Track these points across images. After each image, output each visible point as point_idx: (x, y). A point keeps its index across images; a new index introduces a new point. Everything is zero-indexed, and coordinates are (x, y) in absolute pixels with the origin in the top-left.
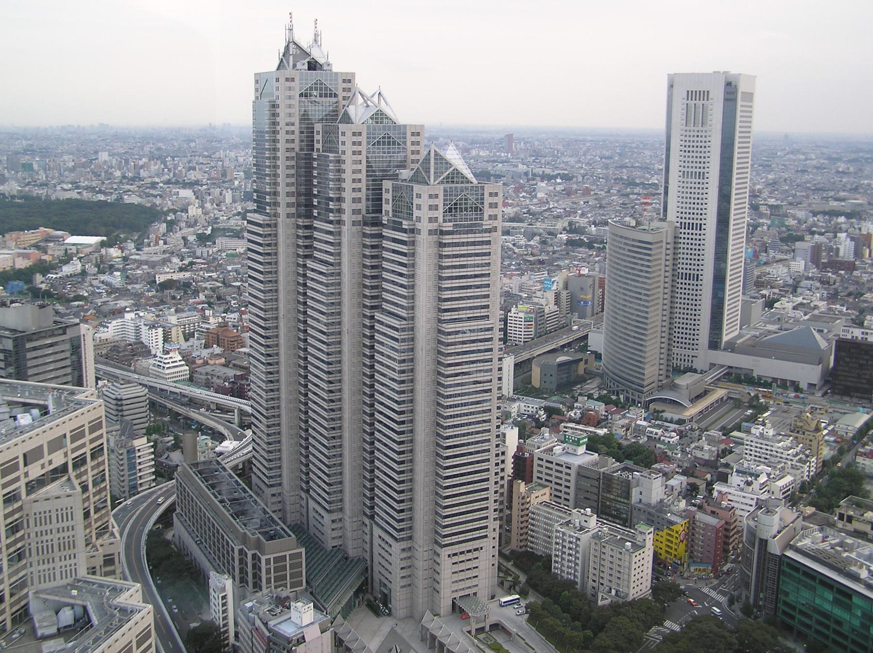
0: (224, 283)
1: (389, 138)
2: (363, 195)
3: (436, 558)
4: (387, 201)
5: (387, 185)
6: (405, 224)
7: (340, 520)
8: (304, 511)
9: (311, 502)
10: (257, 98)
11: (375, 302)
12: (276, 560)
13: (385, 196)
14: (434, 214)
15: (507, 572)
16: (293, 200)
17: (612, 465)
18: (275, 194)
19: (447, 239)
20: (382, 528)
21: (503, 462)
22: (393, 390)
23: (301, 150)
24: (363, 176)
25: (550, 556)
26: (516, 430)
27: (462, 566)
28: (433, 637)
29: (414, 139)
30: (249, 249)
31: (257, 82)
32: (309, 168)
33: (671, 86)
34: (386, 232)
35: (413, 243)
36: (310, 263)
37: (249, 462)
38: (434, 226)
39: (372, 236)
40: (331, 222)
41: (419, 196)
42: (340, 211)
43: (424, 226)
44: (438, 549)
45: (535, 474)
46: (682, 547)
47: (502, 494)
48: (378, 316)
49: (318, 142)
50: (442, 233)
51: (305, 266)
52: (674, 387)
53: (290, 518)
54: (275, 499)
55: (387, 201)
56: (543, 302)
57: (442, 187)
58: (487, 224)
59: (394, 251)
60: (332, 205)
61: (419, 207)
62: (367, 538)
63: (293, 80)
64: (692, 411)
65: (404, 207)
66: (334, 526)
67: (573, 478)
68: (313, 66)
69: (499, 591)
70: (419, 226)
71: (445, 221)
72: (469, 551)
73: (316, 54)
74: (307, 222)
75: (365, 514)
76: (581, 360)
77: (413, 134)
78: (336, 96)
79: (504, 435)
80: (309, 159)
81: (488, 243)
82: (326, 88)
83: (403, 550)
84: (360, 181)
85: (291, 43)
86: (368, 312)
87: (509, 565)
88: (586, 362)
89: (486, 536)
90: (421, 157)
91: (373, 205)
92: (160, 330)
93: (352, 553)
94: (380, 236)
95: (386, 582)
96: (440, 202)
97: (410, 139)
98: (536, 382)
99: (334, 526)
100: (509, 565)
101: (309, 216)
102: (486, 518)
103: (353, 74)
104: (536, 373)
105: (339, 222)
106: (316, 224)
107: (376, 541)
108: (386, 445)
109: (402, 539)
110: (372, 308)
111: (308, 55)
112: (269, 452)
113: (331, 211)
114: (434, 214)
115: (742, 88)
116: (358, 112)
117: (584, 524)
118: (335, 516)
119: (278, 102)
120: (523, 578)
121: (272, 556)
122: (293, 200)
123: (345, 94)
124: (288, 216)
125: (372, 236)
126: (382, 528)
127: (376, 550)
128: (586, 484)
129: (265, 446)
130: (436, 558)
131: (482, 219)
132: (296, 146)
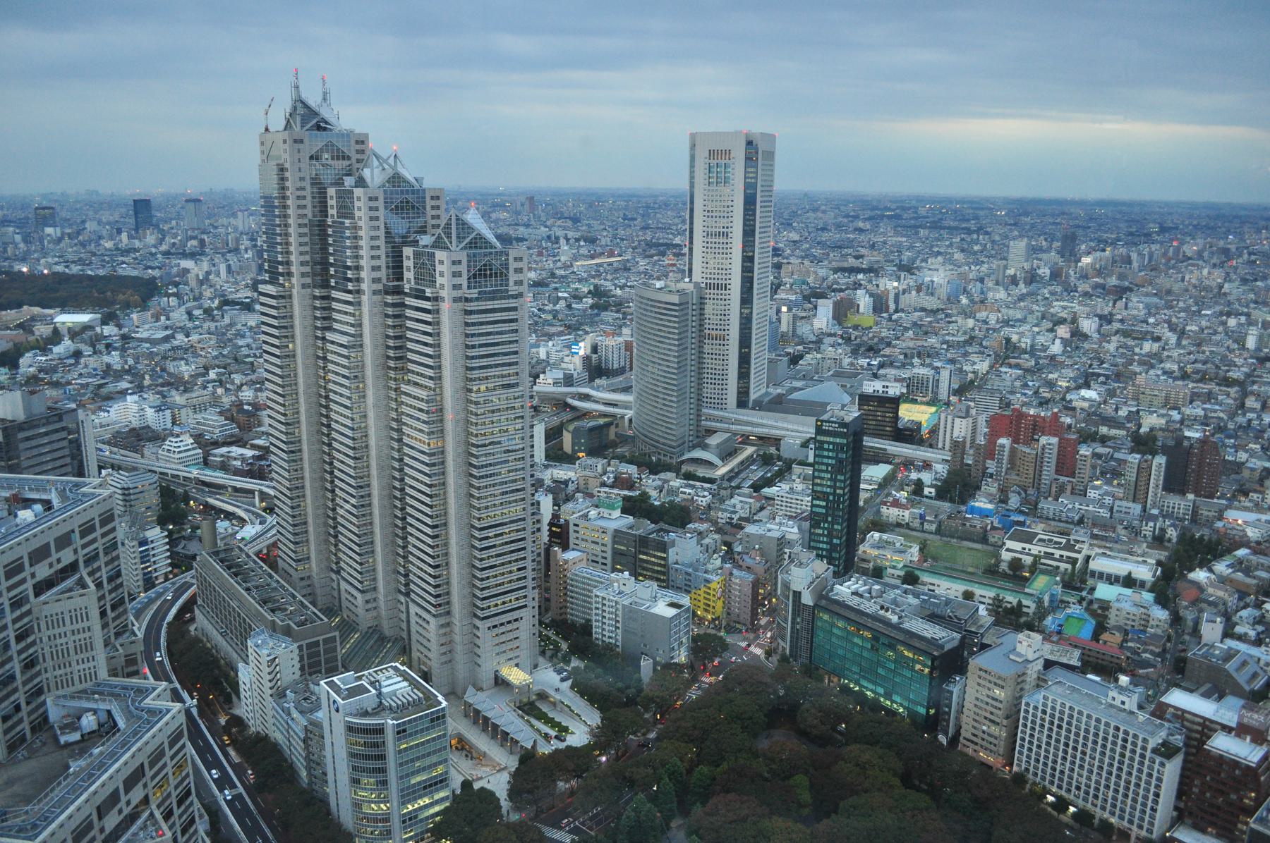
0: (236, 359)
2: (382, 262)
4: (408, 269)
5: (408, 251)
6: (429, 292)
7: (375, 600)
8: (336, 594)
9: (343, 584)
10: (263, 161)
12: (309, 646)
13: (406, 263)
14: (457, 281)
16: (307, 269)
17: (647, 527)
18: (288, 263)
19: (473, 306)
20: (418, 605)
21: (539, 530)
22: (423, 463)
23: (314, 216)
24: (381, 242)
25: (590, 620)
26: (550, 497)
27: (503, 638)
28: (477, 712)
29: (434, 203)
30: (263, 323)
31: (262, 143)
32: (323, 236)
33: (693, 147)
34: (409, 301)
35: (438, 311)
36: (329, 336)
37: (275, 545)
38: (458, 293)
39: (394, 305)
40: (349, 292)
41: (441, 262)
42: (358, 280)
44: (478, 623)
45: (572, 540)
46: (720, 603)
47: (539, 562)
48: (404, 388)
49: (332, 207)
50: (467, 300)
51: (324, 339)
52: (705, 447)
53: (321, 601)
54: (304, 583)
55: (409, 268)
56: (571, 366)
57: (465, 253)
58: (513, 289)
59: (418, 320)
60: (350, 274)
61: (442, 274)
62: (404, 617)
63: (301, 141)
65: (426, 273)
66: (369, 606)
68: (321, 126)
69: (541, 660)
70: (444, 293)
71: (469, 288)
73: (325, 113)
74: (324, 292)
75: (400, 592)
77: (432, 198)
78: (349, 158)
79: (538, 503)
80: (322, 226)
81: (515, 309)
82: (338, 150)
83: (442, 626)
84: (378, 248)
85: (300, 102)
90: (443, 222)
91: (394, 274)
92: (168, 412)
93: (387, 632)
94: (403, 305)
95: (426, 660)
96: (463, 268)
97: (429, 203)
98: (567, 446)
99: (369, 606)
100: (551, 633)
101: (325, 284)
102: (525, 587)
103: (366, 136)
104: (567, 438)
105: (358, 292)
106: (335, 294)
107: (413, 619)
108: (418, 520)
109: (440, 615)
111: (316, 114)
112: (295, 534)
113: (350, 280)
114: (457, 281)
116: (374, 175)
117: (623, 588)
118: (369, 596)
119: (287, 165)
120: (564, 646)
121: (304, 643)
122: (307, 269)
123: (359, 156)
124: (304, 286)
125: (394, 305)
126: (418, 605)
127: (414, 627)
129: (290, 529)
131: (507, 285)
132: (309, 212)
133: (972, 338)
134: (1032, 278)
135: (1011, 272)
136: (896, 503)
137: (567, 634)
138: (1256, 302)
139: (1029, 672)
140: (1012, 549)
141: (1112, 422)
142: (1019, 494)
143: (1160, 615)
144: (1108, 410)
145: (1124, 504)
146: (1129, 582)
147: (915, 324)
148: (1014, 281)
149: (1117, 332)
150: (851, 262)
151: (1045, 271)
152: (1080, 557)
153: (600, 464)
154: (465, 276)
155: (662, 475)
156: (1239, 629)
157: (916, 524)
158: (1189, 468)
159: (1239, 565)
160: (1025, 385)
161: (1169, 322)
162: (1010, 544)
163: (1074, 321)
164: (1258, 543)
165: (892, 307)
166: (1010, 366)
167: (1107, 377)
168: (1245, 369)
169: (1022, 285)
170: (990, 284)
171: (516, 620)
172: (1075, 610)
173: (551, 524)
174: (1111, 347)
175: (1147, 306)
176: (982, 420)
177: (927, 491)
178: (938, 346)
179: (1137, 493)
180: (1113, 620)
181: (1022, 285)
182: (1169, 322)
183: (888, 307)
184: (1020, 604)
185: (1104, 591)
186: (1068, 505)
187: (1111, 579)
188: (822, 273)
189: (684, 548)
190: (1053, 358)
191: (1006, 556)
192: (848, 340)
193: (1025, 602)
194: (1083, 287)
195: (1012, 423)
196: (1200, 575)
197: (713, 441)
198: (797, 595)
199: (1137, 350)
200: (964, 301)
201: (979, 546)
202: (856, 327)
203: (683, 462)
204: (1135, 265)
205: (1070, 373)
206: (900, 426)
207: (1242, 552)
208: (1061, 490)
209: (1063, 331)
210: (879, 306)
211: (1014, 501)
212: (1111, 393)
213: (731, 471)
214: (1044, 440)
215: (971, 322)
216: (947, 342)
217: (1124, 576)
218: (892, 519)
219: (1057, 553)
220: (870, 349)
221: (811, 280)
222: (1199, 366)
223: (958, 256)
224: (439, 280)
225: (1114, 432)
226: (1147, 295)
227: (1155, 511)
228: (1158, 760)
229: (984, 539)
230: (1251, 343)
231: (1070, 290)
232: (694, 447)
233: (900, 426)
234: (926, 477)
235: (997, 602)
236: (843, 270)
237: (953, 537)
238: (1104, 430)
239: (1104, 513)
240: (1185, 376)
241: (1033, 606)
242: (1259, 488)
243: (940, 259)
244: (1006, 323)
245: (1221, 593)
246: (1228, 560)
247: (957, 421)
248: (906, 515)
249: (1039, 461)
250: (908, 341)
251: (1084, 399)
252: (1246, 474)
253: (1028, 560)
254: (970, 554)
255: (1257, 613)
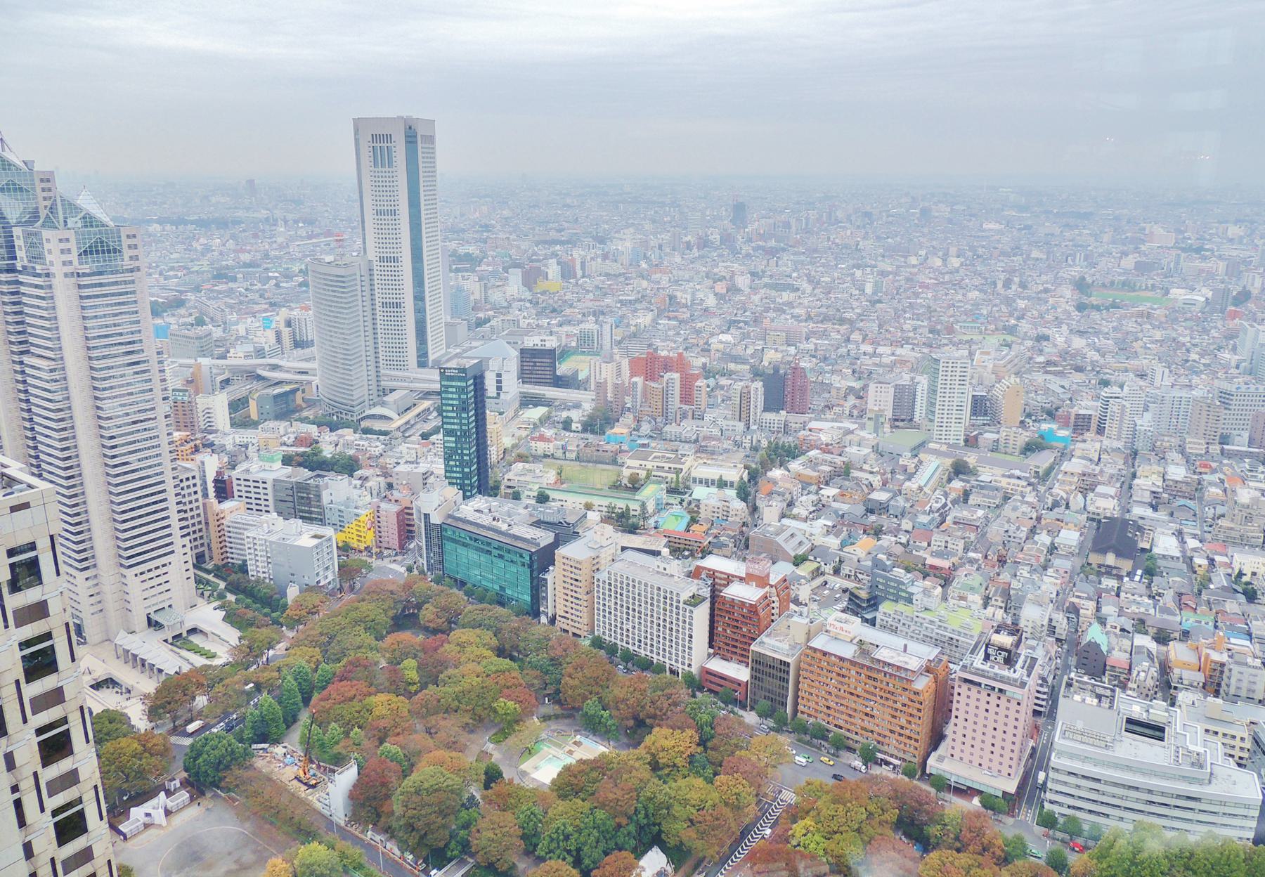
1: (14, 184)
3: (123, 580)
11: (23, 348)
13: (17, 243)
14: (66, 257)
15: (208, 582)
17: (304, 474)
33: (356, 131)
34: (22, 278)
35: (50, 287)
38: (69, 269)
41: (48, 241)
43: (58, 270)
48: (26, 359)
52: (383, 404)
56: (263, 340)
58: (128, 264)
64: (399, 422)
67: (270, 491)
69: (200, 601)
70: (52, 270)
72: (157, 568)
76: (298, 389)
77: (42, 180)
86: (16, 358)
87: (210, 577)
88: (303, 391)
89: (173, 552)
96: (73, 245)
110: (22, 353)
115: (421, 132)
117: (272, 528)
120: (222, 585)
128: (283, 495)
130: (123, 580)
133: (643, 297)
134: (704, 243)
135: (689, 238)
136: (542, 438)
137: (224, 574)
138: (883, 256)
139: (602, 556)
140: (632, 465)
141: (737, 359)
142: (650, 422)
143: (738, 505)
144: (739, 350)
145: (731, 423)
146: (722, 484)
147: (597, 287)
148: (689, 246)
149: (766, 286)
150: (553, 234)
151: (715, 238)
152: (685, 468)
153: (282, 426)
154: (75, 253)
155: (340, 432)
156: (795, 511)
157: (559, 454)
158: (783, 390)
159: (813, 464)
160: (678, 334)
161: (808, 276)
162: (629, 462)
163: (732, 277)
164: (827, 445)
165: (579, 273)
166: (669, 319)
167: (746, 323)
168: (858, 311)
169: (695, 250)
170: (668, 250)
171: (164, 565)
172: (677, 509)
173: (216, 481)
174: (756, 298)
175: (795, 262)
176: (625, 364)
177: (574, 426)
178: (613, 304)
179: (743, 413)
180: (703, 515)
181: (695, 250)
182: (808, 276)
183: (575, 274)
184: (628, 509)
185: (699, 492)
186: (688, 428)
187: (707, 483)
188: (524, 245)
189: (336, 489)
190: (706, 310)
191: (626, 473)
192: (534, 303)
193: (631, 507)
194: (747, 249)
195: (651, 367)
196: (776, 473)
197: (390, 398)
198: (427, 516)
199: (778, 300)
200: (644, 265)
201: (610, 467)
202: (543, 293)
203: (363, 419)
204: (794, 229)
205: (716, 321)
206: (559, 373)
207: (814, 453)
208: (684, 416)
209: (721, 288)
210: (567, 272)
211: (646, 428)
212: (745, 336)
213: (407, 423)
214: (667, 376)
215: (645, 284)
216: (621, 301)
217: (714, 478)
218: (540, 452)
219: (667, 466)
220: (554, 310)
221: (513, 252)
222: (824, 310)
223: (648, 226)
224: (48, 258)
225: (739, 367)
226: (795, 254)
227: (755, 427)
228: (688, 608)
229: (614, 462)
230: (869, 289)
231: (735, 252)
232: (374, 405)
233: (559, 373)
234: (575, 415)
235: (611, 508)
236: (545, 242)
237: (589, 462)
238: (732, 366)
239: (716, 432)
240: (809, 318)
241: (639, 509)
242: (841, 402)
243: (632, 230)
244: (676, 282)
245: (787, 485)
246: (802, 459)
247: (604, 365)
248: (550, 447)
249: (665, 394)
250: (588, 303)
251: (721, 342)
252: (834, 392)
253: (643, 474)
254: (602, 476)
255: (814, 497)
